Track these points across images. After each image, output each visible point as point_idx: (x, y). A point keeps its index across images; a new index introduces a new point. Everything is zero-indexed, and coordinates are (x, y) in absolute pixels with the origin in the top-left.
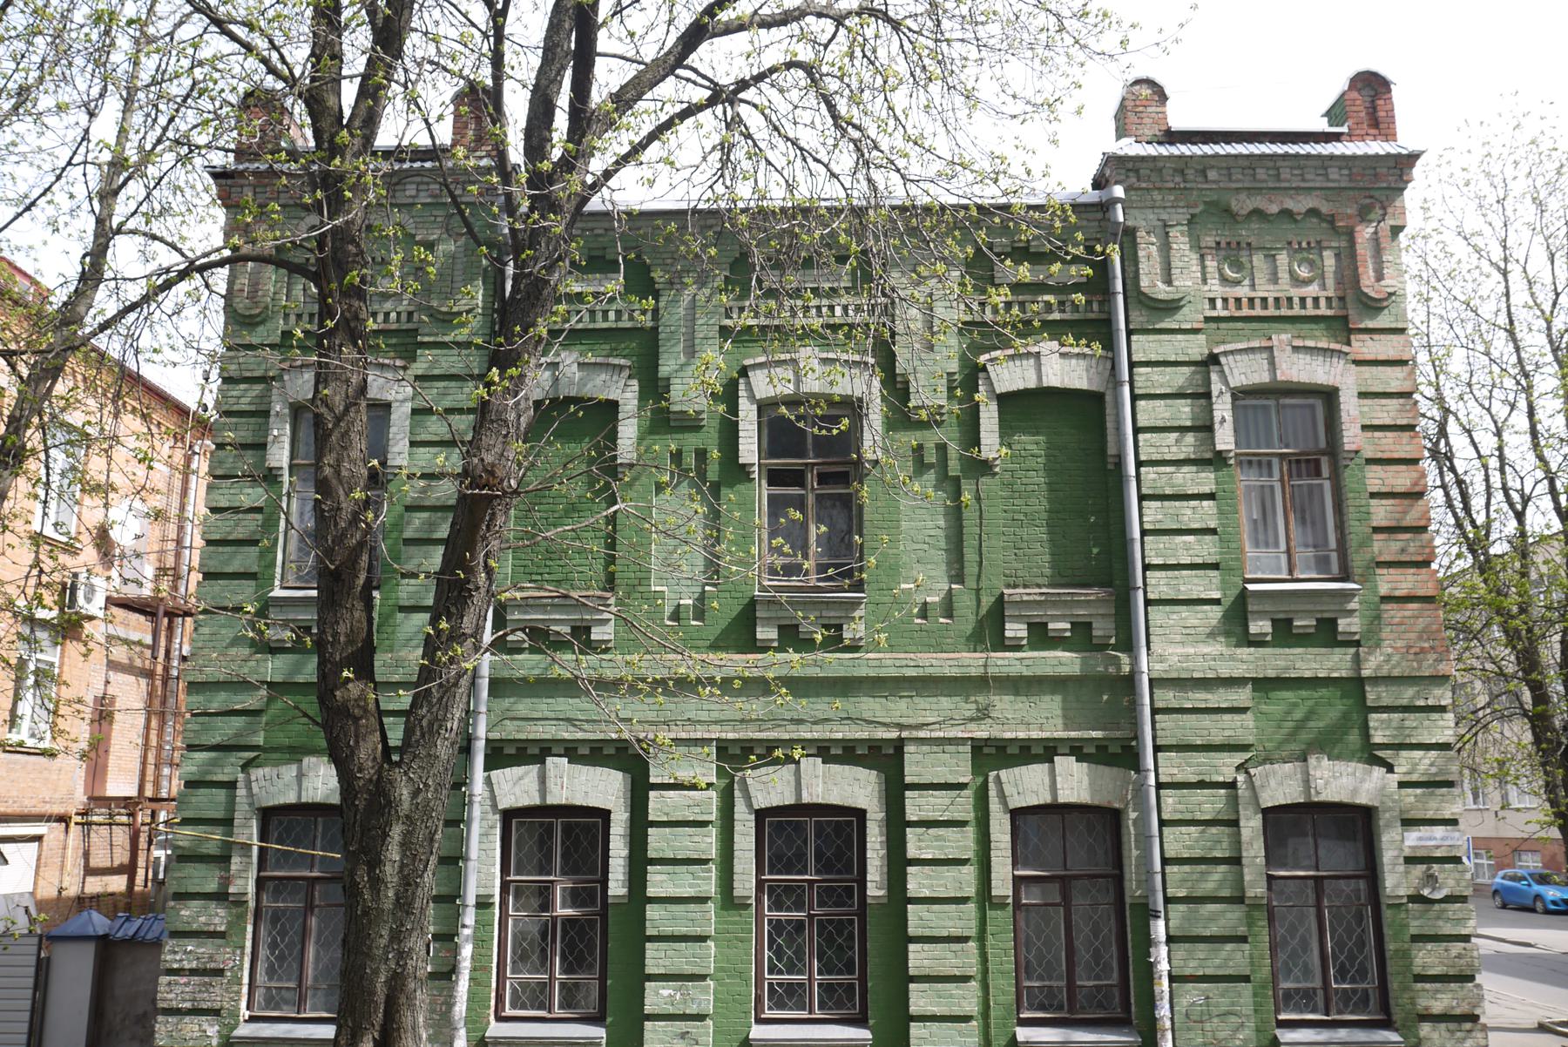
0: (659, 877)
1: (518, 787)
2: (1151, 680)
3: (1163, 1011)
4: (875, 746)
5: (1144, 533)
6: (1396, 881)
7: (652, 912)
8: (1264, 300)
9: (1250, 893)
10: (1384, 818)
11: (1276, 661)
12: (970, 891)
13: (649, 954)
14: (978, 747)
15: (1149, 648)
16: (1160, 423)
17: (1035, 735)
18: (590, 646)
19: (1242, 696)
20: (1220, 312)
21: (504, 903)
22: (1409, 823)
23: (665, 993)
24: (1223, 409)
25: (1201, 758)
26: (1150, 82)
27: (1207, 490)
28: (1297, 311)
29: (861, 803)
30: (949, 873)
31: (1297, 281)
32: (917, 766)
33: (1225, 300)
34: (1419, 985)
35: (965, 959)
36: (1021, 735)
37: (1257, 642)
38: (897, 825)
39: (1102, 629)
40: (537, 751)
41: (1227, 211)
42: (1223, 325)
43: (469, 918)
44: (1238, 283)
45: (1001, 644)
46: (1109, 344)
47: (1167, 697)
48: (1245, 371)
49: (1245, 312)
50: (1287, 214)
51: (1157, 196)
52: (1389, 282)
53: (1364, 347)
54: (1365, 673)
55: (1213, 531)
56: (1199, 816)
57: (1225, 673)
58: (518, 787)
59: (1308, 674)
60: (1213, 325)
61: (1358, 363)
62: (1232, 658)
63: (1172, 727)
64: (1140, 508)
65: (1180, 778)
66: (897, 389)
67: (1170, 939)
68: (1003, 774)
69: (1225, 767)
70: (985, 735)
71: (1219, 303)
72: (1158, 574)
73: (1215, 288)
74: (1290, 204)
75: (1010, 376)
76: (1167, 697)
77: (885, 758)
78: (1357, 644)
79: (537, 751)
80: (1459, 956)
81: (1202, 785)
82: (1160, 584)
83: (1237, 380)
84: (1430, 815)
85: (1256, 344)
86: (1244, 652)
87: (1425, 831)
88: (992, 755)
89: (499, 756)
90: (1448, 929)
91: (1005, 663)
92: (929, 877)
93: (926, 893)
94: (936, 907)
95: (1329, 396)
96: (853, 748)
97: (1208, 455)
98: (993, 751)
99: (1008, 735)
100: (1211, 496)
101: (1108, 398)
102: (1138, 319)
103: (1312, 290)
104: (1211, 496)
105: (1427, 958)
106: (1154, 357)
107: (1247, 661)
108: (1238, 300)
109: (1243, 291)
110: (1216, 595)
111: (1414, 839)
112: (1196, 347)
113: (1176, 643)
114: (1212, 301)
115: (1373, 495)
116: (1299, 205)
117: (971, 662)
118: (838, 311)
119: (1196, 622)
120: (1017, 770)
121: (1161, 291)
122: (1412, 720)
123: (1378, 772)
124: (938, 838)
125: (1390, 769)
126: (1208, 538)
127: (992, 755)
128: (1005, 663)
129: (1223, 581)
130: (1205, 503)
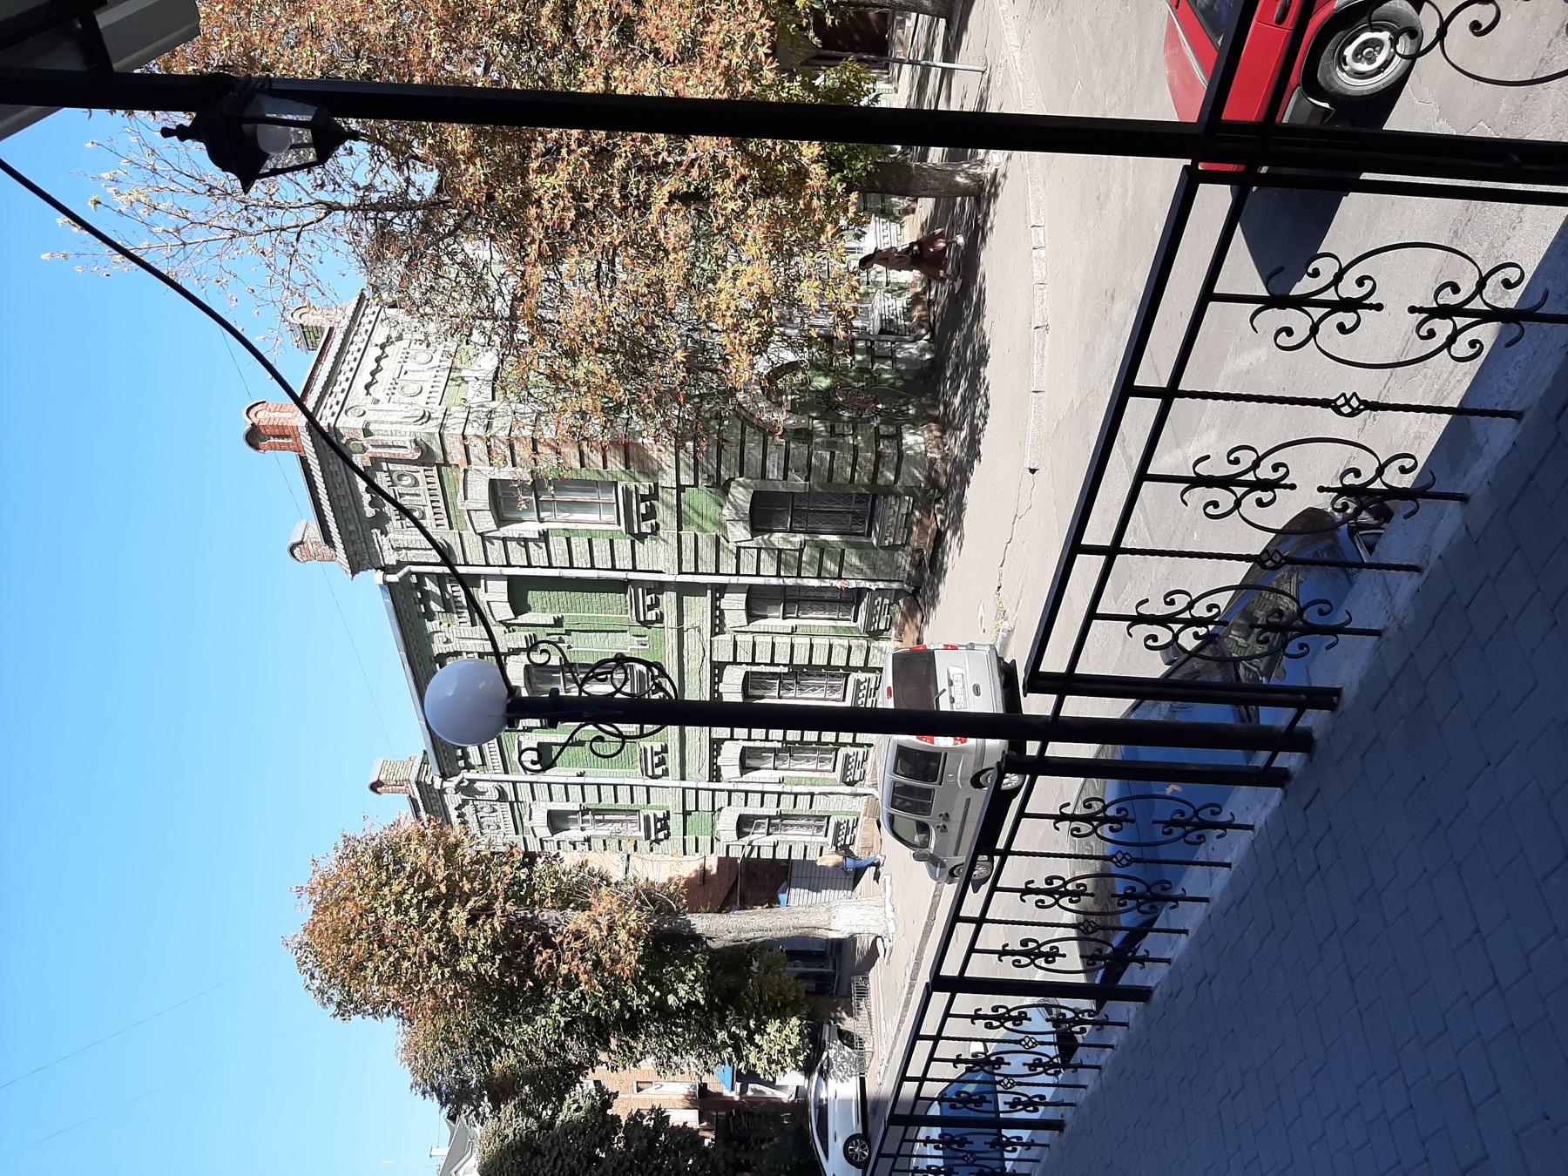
1: (730, 770)
5: (593, 567)
11: (665, 516)
12: (787, 639)
14: (714, 634)
18: (665, 749)
20: (446, 521)
22: (763, 476)
24: (511, 530)
28: (437, 485)
31: (416, 483)
32: (724, 655)
37: (655, 529)
43: (787, 789)
45: (660, 618)
46: (478, 576)
47: (688, 566)
48: (486, 522)
52: (406, 440)
53: (456, 456)
55: (590, 541)
58: (730, 770)
61: (469, 462)
76: (688, 566)
82: (624, 561)
89: (715, 774)
95: (492, 482)
100: (568, 540)
103: (420, 477)
104: (568, 540)
107: (668, 531)
113: (658, 559)
127: (718, 627)
128: (670, 619)
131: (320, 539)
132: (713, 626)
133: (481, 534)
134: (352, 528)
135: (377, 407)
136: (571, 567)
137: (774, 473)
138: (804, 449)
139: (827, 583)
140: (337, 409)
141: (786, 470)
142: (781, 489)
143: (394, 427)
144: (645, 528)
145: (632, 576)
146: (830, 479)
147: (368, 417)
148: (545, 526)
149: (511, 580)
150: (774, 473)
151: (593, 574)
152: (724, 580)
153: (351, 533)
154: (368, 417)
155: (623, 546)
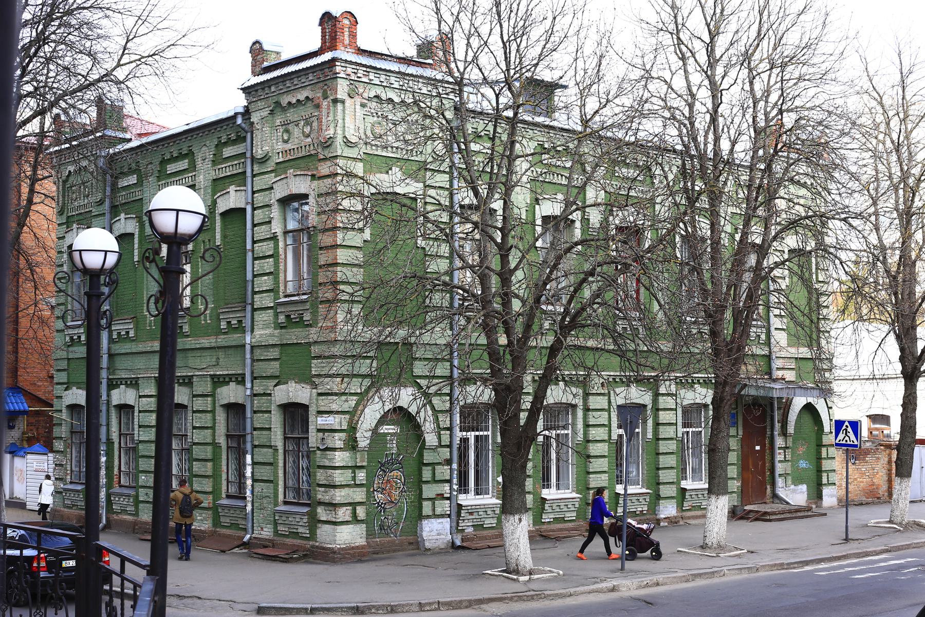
2: (252, 347)
3: (248, 493)
5: (254, 276)
6: (314, 439)
7: (141, 447)
10: (312, 410)
14: (213, 377)
19: (274, 353)
21: (120, 443)
22: (320, 413)
25: (265, 382)
26: (254, 43)
27: (271, 253)
44: (286, 142)
49: (289, 157)
51: (259, 103)
60: (279, 166)
61: (320, 178)
64: (253, 264)
65: (258, 392)
67: (254, 463)
70: (212, 373)
76: (258, 354)
80: (330, 476)
83: (279, 195)
88: (219, 381)
90: (327, 463)
105: (321, 476)
106: (259, 188)
116: (301, 97)
119: (265, 318)
124: (200, 418)
128: (222, 340)
131: (266, 64)
133: (272, 188)
135: (358, 107)
136: (255, 259)
137: (322, 421)
138: (339, 444)
140: (353, 77)
142: (310, 427)
143: (340, 121)
144: (282, 318)
145: (249, 308)
146: (320, 467)
147: (349, 102)
148: (281, 238)
149: (244, 210)
150: (322, 421)
151: (249, 276)
152: (249, 385)
154: (349, 102)
155: (266, 300)
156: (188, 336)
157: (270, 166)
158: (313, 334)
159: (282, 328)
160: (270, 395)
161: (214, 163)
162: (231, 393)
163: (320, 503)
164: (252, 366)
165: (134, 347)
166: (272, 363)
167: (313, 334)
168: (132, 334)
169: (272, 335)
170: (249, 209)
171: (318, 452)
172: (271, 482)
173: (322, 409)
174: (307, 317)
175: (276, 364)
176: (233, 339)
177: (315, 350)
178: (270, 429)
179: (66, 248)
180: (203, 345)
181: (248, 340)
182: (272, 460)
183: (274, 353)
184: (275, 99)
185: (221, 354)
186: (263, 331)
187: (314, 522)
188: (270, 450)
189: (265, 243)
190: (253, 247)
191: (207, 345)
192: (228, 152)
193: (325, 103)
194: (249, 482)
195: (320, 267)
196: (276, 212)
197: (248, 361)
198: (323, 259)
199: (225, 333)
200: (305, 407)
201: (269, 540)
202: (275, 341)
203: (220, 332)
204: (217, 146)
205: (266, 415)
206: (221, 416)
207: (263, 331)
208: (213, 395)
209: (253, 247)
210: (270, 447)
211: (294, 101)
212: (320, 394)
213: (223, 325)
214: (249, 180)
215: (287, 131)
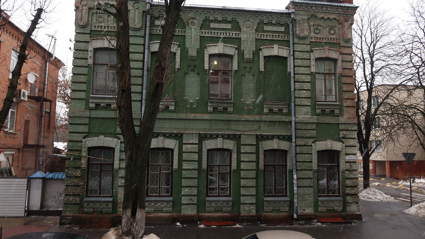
0: (185, 164)
2: (295, 123)
4: (235, 135)
5: (295, 90)
6: (343, 166)
7: (183, 172)
8: (323, 38)
9: (314, 168)
10: (343, 153)
13: (183, 181)
14: (257, 136)
15: (295, 115)
16: (300, 65)
17: (270, 134)
22: (346, 154)
23: (187, 190)
25: (305, 140)
27: (309, 81)
29: (231, 148)
30: (251, 164)
33: (314, 38)
34: (346, 188)
35: (253, 183)
36: (267, 134)
38: (239, 153)
39: (285, 111)
40: (156, 135)
41: (316, 17)
42: (314, 43)
44: (317, 34)
50: (328, 18)
54: (340, 122)
56: (304, 152)
57: (311, 121)
59: (328, 122)
60: (312, 43)
62: (313, 118)
63: (300, 133)
64: (295, 84)
66: (241, 54)
68: (263, 142)
69: (310, 141)
70: (259, 134)
71: (313, 38)
72: (298, 99)
73: (312, 34)
74: (330, 17)
75: (266, 52)
76: (299, 126)
77: (236, 138)
78: (338, 116)
79: (156, 135)
81: (305, 145)
82: (298, 101)
84: (351, 153)
85: (321, 48)
86: (315, 117)
87: (350, 156)
88: (260, 138)
90: (353, 176)
91: (264, 118)
92: (245, 165)
93: (245, 168)
94: (247, 171)
96: (230, 136)
97: (309, 73)
98: (260, 137)
99: (264, 134)
101: (288, 59)
102: (296, 40)
103: (334, 36)
106: (299, 50)
107: (315, 119)
108: (317, 38)
109: (319, 36)
110: (310, 104)
111: (348, 158)
112: (308, 48)
114: (312, 37)
115: (343, 83)
117: (257, 118)
118: (228, 34)
120: (265, 142)
121: (302, 35)
122: (348, 133)
123: (341, 143)
125: (343, 143)
126: (309, 92)
127: (260, 138)
128: (264, 118)
129: (311, 101)
130: (308, 84)
132: (262, 136)
134: (314, 8)
136: (295, 82)
139: (295, 182)
141: (350, 162)
151: (292, 89)
152: (294, 140)
153: (311, 7)
156: (231, 114)
157: (307, 41)
158: (342, 120)
159: (317, 115)
160: (311, 146)
161: (256, 31)
162: (274, 144)
163: (348, 195)
164: (295, 132)
165: (174, 116)
166: (311, 131)
167: (342, 120)
168: (172, 108)
169: (310, 118)
170: (292, 57)
171: (347, 172)
172: (312, 187)
173: (349, 153)
174: (337, 111)
175: (315, 132)
176: (284, 118)
177: (341, 127)
178: (311, 162)
179: (90, 48)
180: (248, 119)
181: (293, 119)
182: (312, 177)
183: (314, 126)
184: (313, 13)
185: (262, 125)
186: (303, 115)
187: (345, 204)
188: (311, 172)
189: (304, 76)
190: (294, 76)
191: (252, 119)
192: (266, 28)
193: (346, 23)
194: (295, 188)
195: (344, 91)
196: (313, 63)
197: (293, 130)
198: (345, 88)
199: (267, 115)
200: (337, 153)
201: (313, 215)
202: (315, 121)
203: (261, 113)
204: (259, 23)
205: (310, 155)
206: (262, 156)
207: (303, 115)
208: (257, 146)
209: (294, 76)
210: (311, 170)
211: (326, 17)
212: (346, 146)
213: (266, 110)
214: (291, 45)
215: (317, 29)
